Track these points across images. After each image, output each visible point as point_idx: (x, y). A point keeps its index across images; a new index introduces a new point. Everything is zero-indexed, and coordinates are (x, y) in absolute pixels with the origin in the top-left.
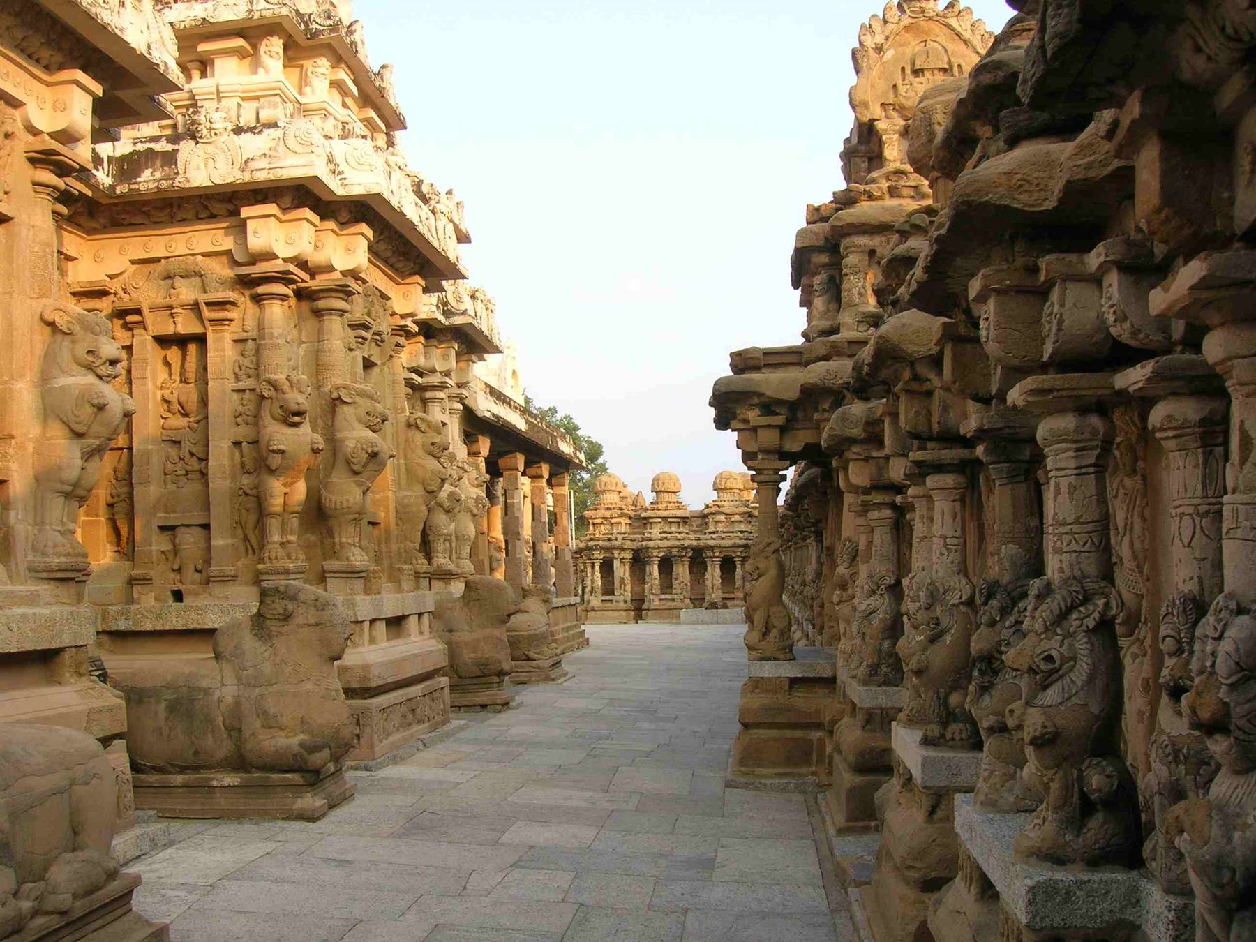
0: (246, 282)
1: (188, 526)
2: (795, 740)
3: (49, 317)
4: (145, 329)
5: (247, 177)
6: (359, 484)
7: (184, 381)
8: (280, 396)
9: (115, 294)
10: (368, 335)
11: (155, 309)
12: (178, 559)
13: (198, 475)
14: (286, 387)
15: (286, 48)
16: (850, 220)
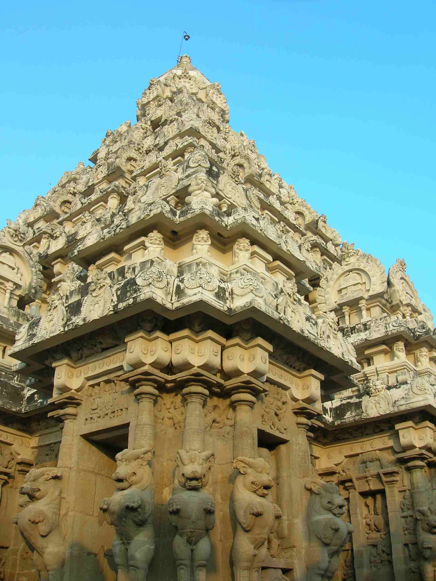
0: (402, 461)
3: (309, 486)
4: (355, 489)
5: (396, 410)
7: (376, 514)
8: (426, 518)
9: (339, 473)
11: (358, 479)
13: (387, 563)
14: (429, 514)
15: (406, 346)
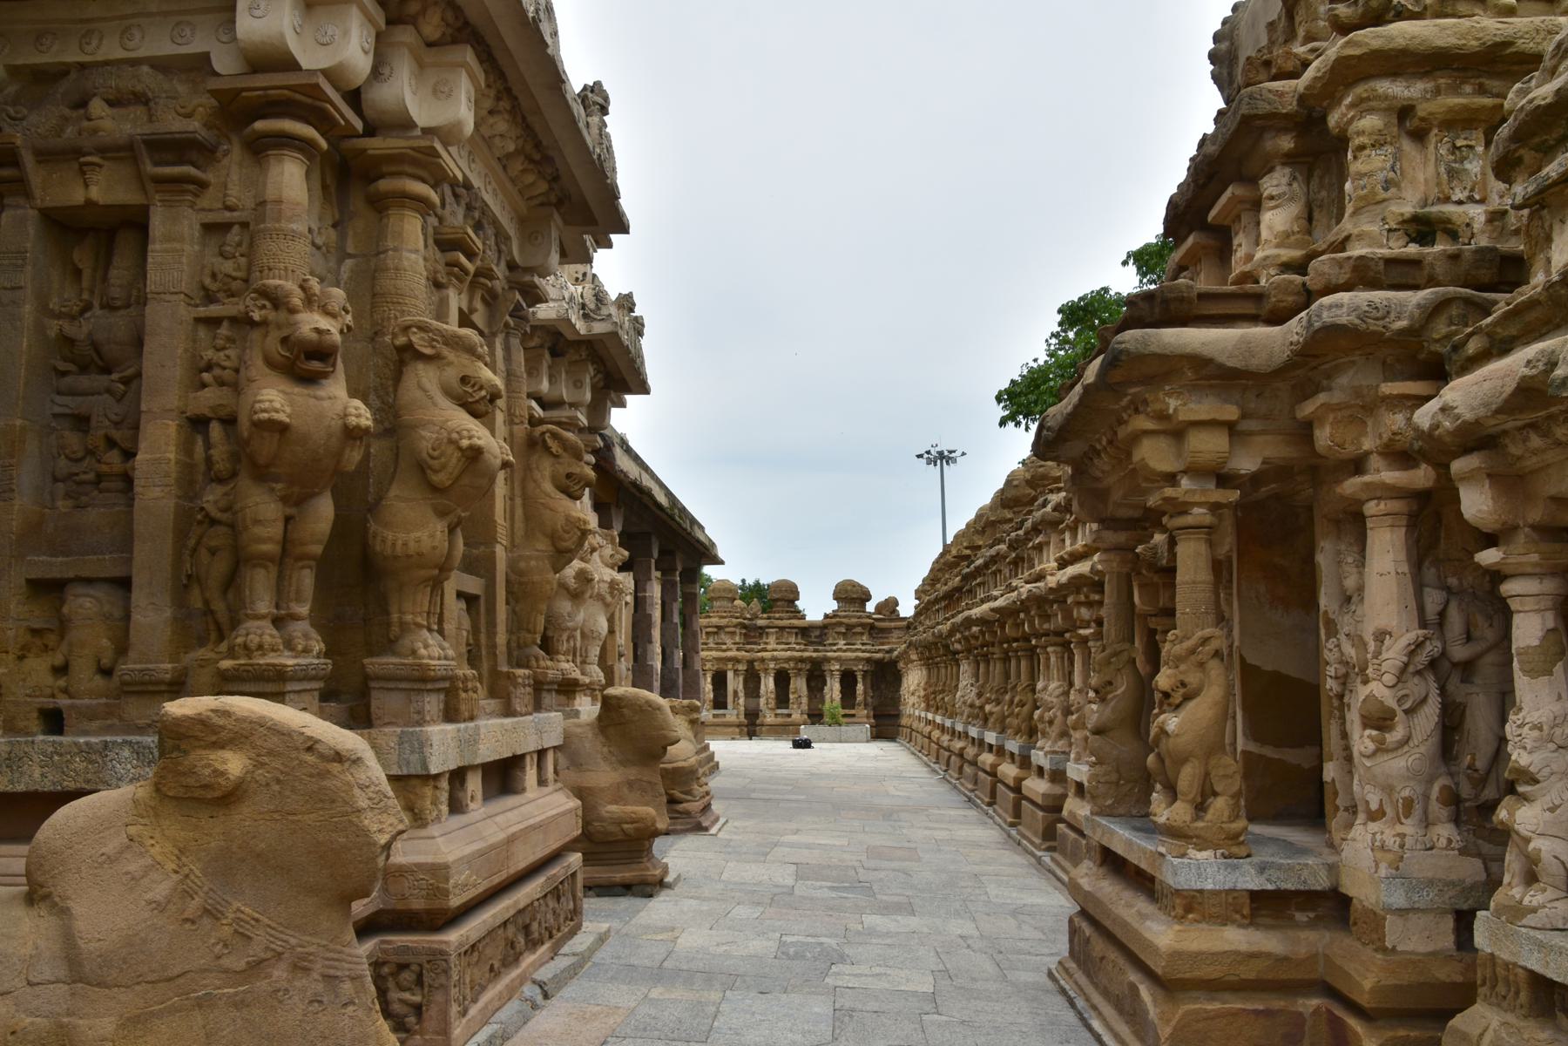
1: (89, 581)
2: (1267, 1013)
6: (441, 513)
8: (282, 315)
10: (471, 267)
12: (64, 647)
14: (297, 301)
16: (1376, 44)
